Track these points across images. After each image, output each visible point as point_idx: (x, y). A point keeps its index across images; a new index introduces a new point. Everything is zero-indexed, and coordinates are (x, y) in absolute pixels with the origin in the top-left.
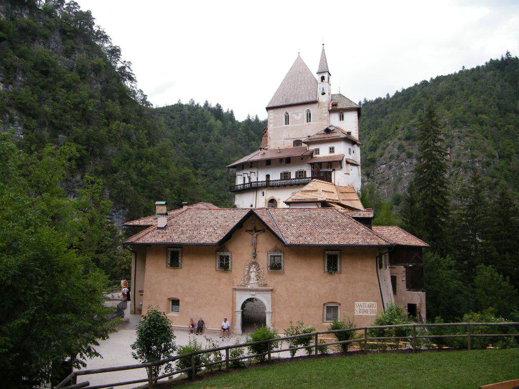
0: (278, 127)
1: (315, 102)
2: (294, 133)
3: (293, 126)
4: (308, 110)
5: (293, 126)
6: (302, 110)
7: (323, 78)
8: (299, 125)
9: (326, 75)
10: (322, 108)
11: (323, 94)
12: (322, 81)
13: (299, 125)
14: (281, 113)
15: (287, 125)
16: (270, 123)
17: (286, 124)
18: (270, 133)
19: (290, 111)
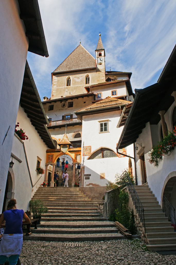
0: (60, 87)
1: (95, 69)
2: (74, 91)
3: (73, 86)
4: (88, 76)
5: (73, 86)
6: (84, 75)
7: (100, 55)
8: (80, 85)
9: (103, 53)
10: (99, 74)
11: (101, 64)
12: (99, 56)
13: (80, 85)
14: (64, 78)
15: (69, 86)
16: (54, 85)
17: (68, 85)
18: (54, 92)
19: (72, 77)
